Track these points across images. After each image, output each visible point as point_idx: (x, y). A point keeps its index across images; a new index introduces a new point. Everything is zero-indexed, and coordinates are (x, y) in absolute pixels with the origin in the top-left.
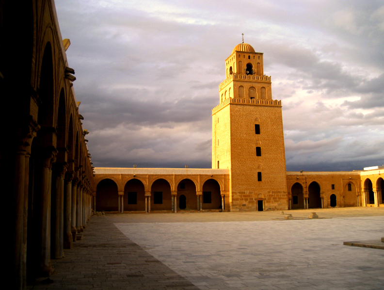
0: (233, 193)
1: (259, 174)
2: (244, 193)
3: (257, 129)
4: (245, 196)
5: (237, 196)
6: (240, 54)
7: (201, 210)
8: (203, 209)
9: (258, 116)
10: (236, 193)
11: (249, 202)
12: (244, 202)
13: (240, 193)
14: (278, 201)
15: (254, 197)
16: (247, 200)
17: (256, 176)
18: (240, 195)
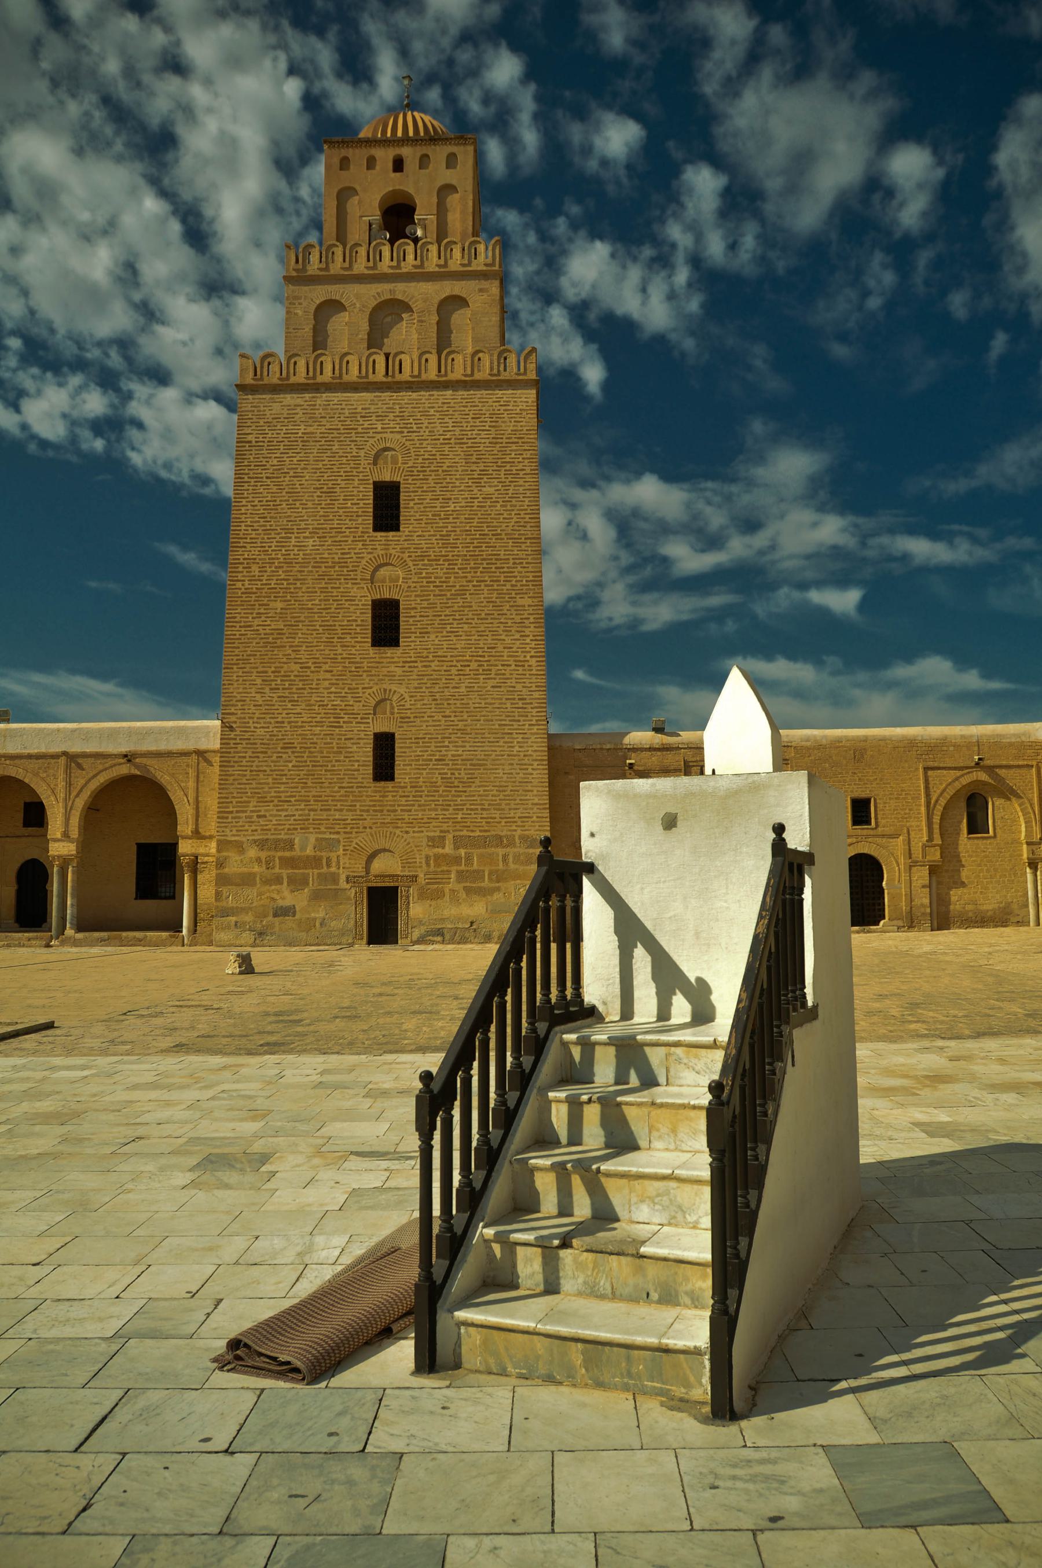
0: (222, 845)
1: (384, 747)
2: (290, 845)
3: (387, 508)
4: (289, 863)
5: (244, 861)
6: (349, 152)
7: (69, 932)
8: (80, 928)
9: (393, 439)
10: (240, 847)
11: (316, 896)
12: (287, 897)
13: (261, 844)
14: (492, 891)
15: (346, 865)
16: (304, 882)
17: (365, 753)
18: (263, 855)
